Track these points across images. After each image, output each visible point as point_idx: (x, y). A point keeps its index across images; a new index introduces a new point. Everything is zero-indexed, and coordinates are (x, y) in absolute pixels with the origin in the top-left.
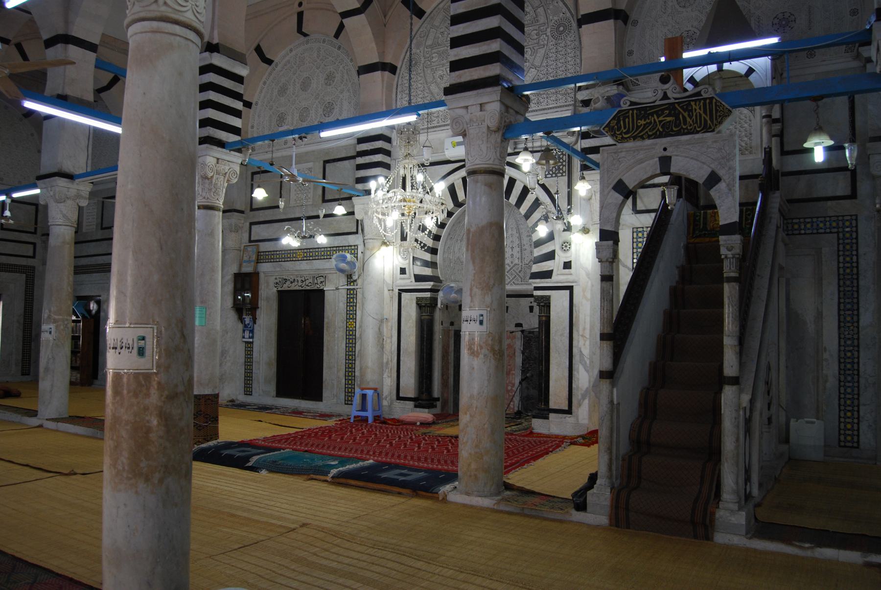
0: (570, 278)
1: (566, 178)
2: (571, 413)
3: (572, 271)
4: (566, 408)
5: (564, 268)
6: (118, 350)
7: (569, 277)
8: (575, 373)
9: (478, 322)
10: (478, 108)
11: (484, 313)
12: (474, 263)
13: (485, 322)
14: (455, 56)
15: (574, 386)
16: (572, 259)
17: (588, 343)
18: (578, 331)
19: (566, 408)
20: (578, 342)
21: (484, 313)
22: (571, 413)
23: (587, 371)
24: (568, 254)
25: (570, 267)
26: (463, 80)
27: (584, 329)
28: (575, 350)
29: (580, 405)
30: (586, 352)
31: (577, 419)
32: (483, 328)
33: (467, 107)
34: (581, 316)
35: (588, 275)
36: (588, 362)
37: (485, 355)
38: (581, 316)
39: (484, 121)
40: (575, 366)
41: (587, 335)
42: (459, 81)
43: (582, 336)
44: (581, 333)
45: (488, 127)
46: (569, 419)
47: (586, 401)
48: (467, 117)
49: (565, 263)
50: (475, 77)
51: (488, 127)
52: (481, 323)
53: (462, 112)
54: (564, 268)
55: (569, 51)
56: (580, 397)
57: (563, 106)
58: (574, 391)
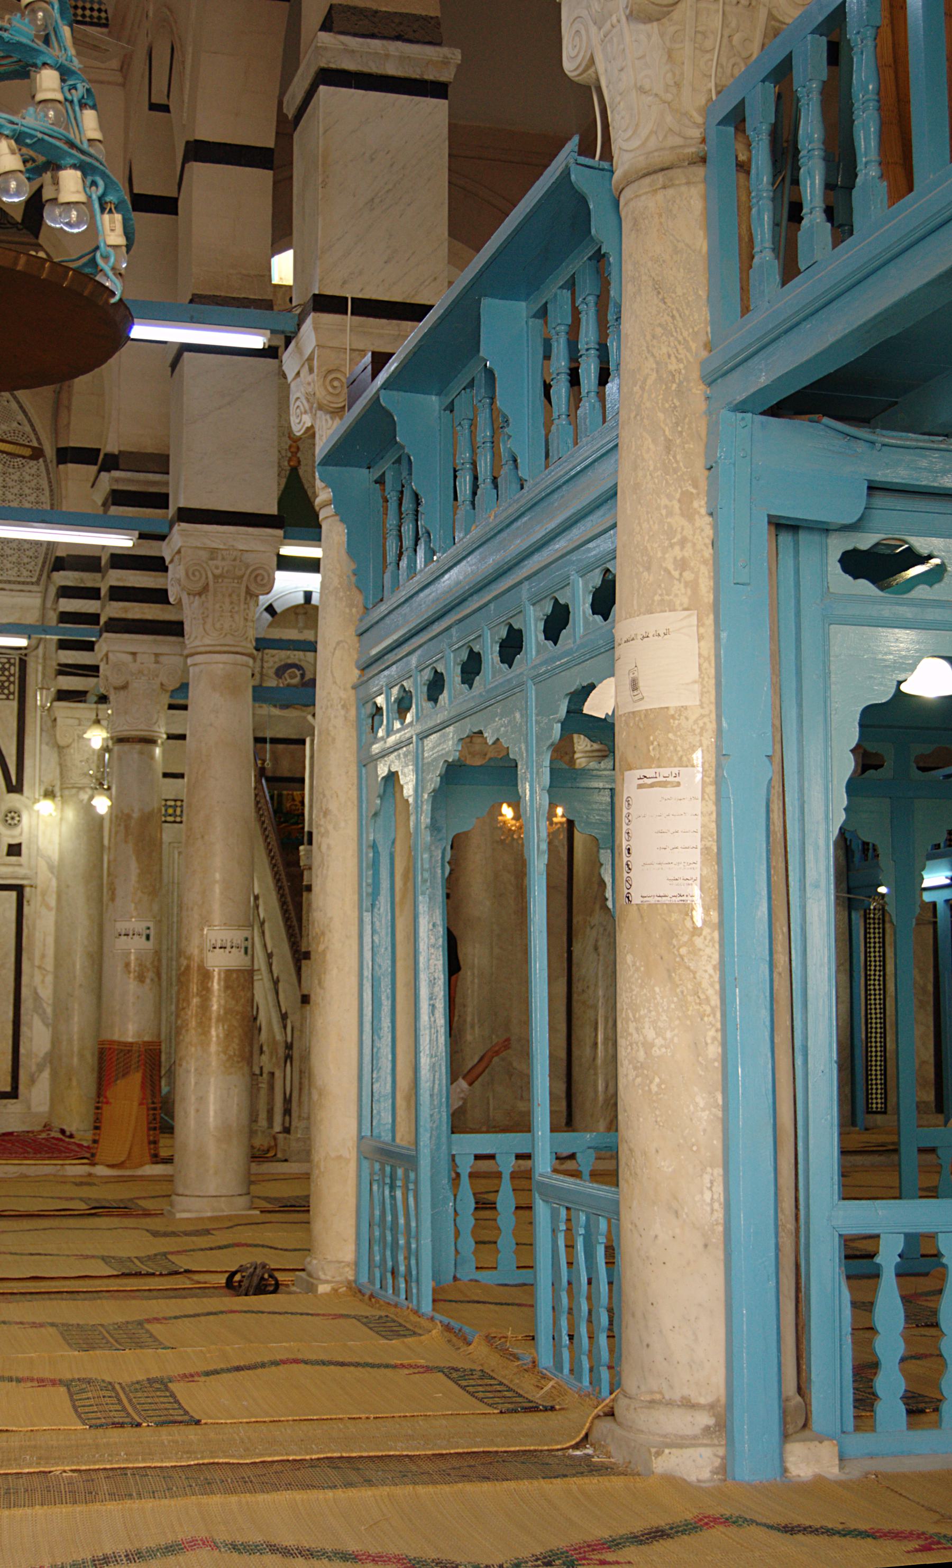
0: (21, 871)
1: (15, 704)
2: (16, 1097)
3: (23, 859)
4: (8, 1089)
5: (9, 854)
6: (228, 949)
7: (17, 869)
8: (24, 1029)
9: (144, 937)
10: (153, 658)
11: (151, 924)
12: (137, 859)
13: (151, 937)
14: (118, 580)
15: (22, 1051)
16: (23, 840)
17: (50, 979)
18: (31, 959)
19: (8, 1089)
20: (32, 977)
21: (151, 924)
22: (16, 1097)
23: (47, 1025)
24: (16, 831)
25: (19, 854)
26: (130, 616)
27: (43, 956)
28: (25, 991)
29: (33, 1081)
30: (46, 993)
31: (29, 1108)
32: (150, 945)
33: (134, 654)
34: (38, 935)
35: (51, 868)
36: (49, 1010)
37: (152, 980)
38: (37, 934)
39: (157, 676)
40: (24, 1018)
41: (49, 964)
42: (123, 616)
43: (39, 967)
44: (37, 963)
45: (162, 684)
46: (12, 1106)
47: (46, 1074)
48: (134, 667)
49: (10, 846)
50: (149, 617)
51: (162, 684)
52: (148, 938)
53: (129, 658)
54: (9, 854)
55: (11, 484)
56: (34, 1068)
57: (14, 582)
58: (22, 1059)
